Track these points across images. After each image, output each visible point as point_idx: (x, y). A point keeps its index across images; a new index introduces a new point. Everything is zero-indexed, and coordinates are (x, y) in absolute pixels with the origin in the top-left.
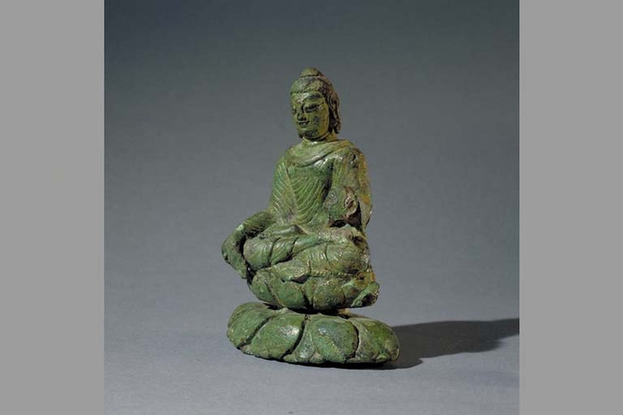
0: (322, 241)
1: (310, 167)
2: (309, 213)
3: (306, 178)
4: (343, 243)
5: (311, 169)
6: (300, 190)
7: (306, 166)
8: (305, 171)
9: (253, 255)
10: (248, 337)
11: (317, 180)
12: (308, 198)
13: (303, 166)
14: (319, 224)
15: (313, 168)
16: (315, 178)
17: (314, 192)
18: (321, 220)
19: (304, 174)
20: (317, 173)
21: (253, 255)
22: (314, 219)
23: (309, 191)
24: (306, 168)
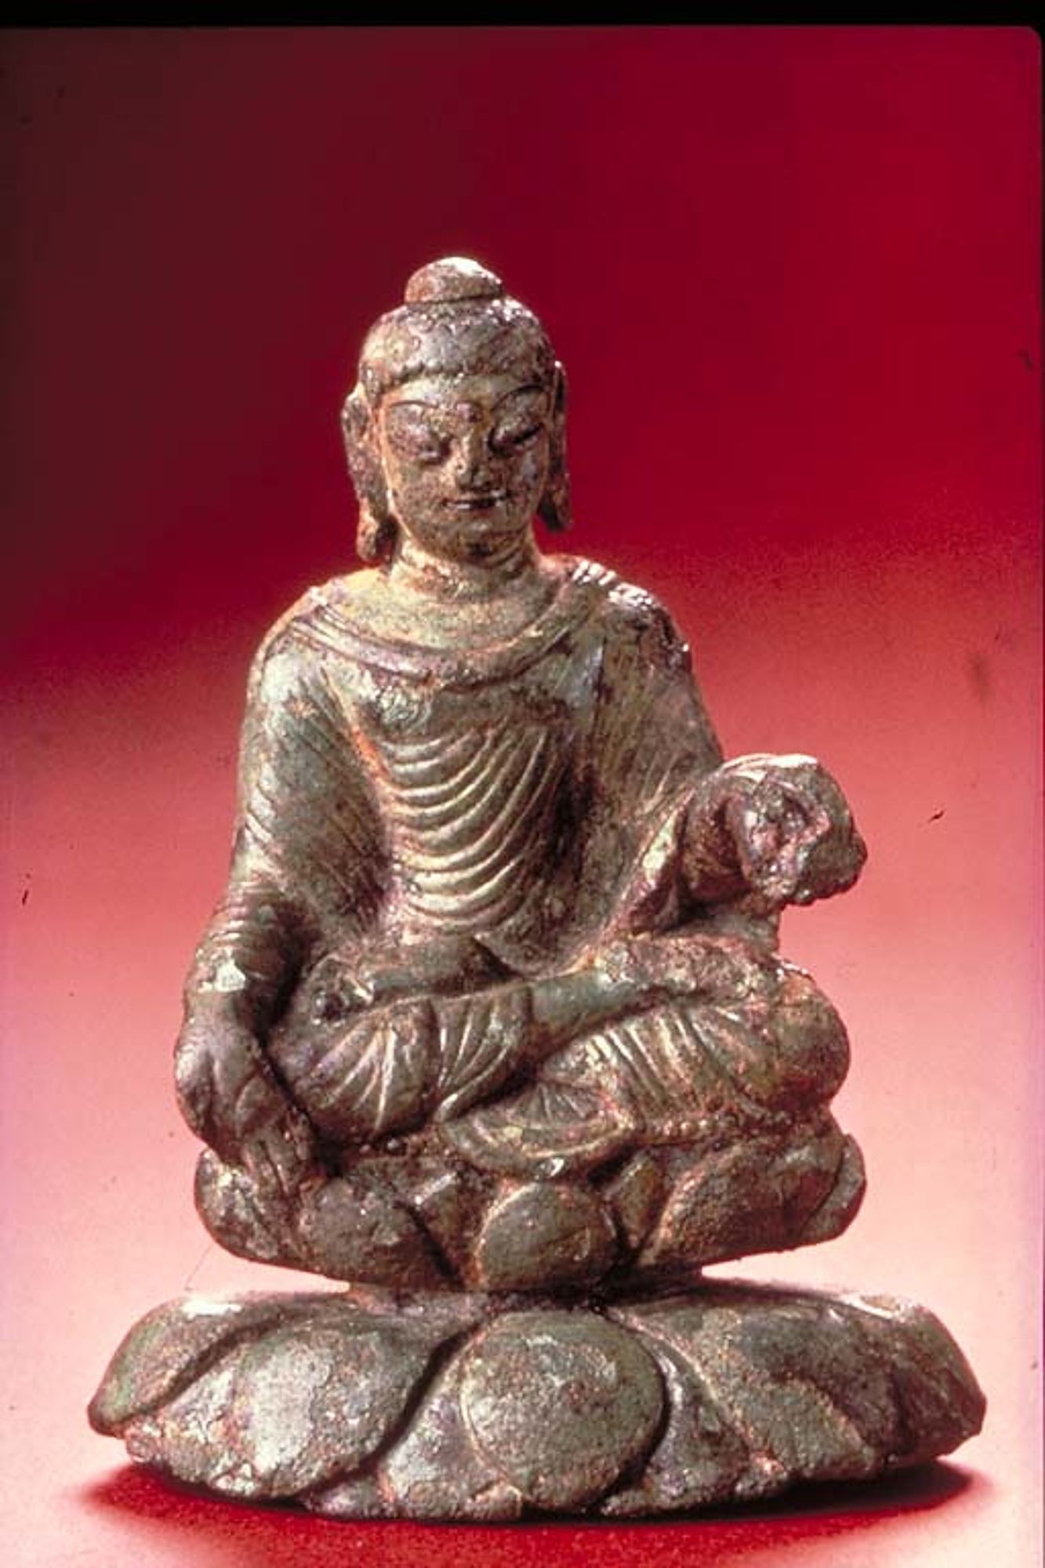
0: (661, 996)
1: (514, 686)
2: (509, 880)
3: (490, 733)
4: (751, 990)
5: (513, 692)
6: (462, 786)
7: (493, 681)
8: (486, 705)
9: (338, 1091)
10: (370, 1446)
11: (541, 741)
12: (502, 817)
13: (477, 686)
14: (554, 922)
15: (523, 692)
16: (531, 730)
17: (532, 786)
18: (558, 907)
19: (483, 716)
20: (539, 708)
21: (338, 1091)
22: (529, 902)
23: (507, 790)
24: (494, 693)
